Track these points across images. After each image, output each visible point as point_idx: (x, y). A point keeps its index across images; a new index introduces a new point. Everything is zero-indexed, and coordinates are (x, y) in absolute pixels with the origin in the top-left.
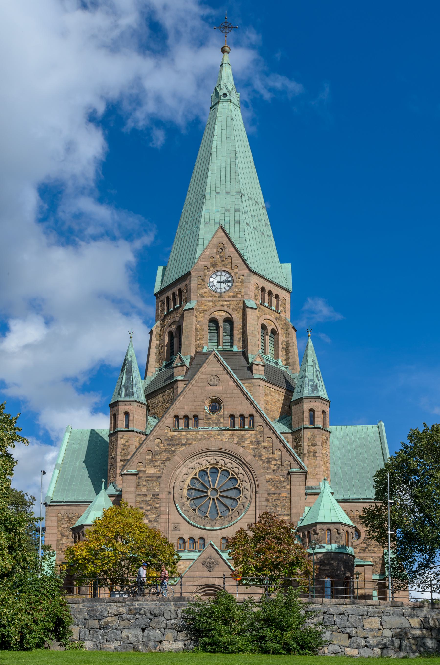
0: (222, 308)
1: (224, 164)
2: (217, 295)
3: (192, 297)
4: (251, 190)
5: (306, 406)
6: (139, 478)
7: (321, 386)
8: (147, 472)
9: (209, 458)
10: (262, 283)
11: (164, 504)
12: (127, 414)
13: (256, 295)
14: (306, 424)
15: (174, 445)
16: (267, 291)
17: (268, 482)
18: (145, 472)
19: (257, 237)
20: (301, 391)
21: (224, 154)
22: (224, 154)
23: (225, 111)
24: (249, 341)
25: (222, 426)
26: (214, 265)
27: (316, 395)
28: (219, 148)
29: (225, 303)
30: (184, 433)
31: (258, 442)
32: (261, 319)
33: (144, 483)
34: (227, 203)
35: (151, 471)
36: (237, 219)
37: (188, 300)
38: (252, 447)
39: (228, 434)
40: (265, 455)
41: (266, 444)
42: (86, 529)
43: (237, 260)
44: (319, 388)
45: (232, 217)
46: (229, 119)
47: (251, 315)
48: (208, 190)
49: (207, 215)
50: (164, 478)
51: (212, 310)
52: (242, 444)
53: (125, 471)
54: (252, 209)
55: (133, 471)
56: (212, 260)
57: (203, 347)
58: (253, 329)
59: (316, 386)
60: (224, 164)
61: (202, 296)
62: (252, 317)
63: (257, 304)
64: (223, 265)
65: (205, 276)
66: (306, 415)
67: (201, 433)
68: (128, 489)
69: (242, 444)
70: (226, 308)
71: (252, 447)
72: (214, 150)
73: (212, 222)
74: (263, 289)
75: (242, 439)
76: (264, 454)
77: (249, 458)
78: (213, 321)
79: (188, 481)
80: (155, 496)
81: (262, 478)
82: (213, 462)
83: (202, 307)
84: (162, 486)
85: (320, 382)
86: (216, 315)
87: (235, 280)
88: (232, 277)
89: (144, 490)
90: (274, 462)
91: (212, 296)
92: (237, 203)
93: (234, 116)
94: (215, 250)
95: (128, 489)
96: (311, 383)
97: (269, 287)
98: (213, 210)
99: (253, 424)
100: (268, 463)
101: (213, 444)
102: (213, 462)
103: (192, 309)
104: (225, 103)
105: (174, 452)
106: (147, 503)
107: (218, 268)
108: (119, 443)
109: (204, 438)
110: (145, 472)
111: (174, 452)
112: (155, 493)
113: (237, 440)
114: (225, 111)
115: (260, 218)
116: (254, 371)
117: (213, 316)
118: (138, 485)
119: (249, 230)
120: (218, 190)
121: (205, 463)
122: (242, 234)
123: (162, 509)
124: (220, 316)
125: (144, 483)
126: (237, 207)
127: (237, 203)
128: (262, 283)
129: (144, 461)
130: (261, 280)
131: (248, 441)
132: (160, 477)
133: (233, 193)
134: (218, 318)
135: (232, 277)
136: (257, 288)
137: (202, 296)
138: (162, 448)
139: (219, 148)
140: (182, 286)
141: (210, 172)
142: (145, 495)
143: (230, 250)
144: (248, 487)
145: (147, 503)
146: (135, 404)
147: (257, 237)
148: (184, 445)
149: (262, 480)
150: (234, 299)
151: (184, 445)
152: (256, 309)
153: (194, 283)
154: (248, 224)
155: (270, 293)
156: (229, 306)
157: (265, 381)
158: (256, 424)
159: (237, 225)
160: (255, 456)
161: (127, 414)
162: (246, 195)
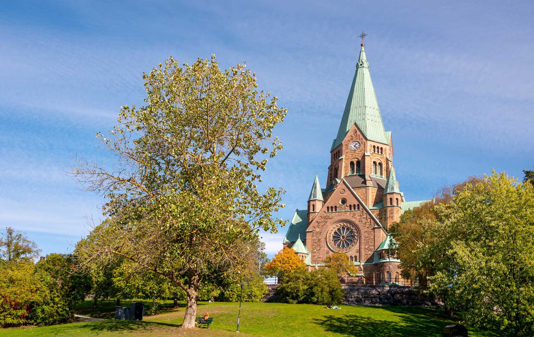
0: (356, 157)
1: (359, 95)
2: (353, 152)
3: (343, 153)
4: (371, 103)
5: (389, 197)
6: (313, 233)
7: (396, 188)
8: (316, 230)
9: (341, 224)
10: (373, 144)
11: (322, 243)
12: (313, 205)
13: (370, 150)
14: (389, 204)
15: (327, 219)
16: (376, 147)
17: (365, 232)
18: (315, 230)
19: (373, 124)
20: (387, 191)
21: (359, 90)
22: (359, 90)
23: (361, 71)
24: (366, 170)
25: (346, 210)
26: (352, 139)
27: (393, 192)
28: (357, 88)
29: (357, 155)
30: (331, 214)
31: (361, 216)
32: (373, 159)
33: (315, 235)
34: (360, 111)
35: (317, 230)
36: (363, 118)
37: (341, 155)
38: (358, 218)
39: (348, 213)
40: (364, 221)
41: (364, 216)
42: (299, 254)
43: (361, 137)
44: (394, 188)
45: (361, 117)
46: (363, 75)
47: (367, 159)
48: (352, 107)
49: (351, 118)
50: (323, 232)
51: (351, 158)
52: (354, 217)
53: (307, 231)
54: (371, 112)
55: (311, 230)
56: (351, 137)
57: (347, 174)
58: (368, 164)
59: (393, 187)
60: (359, 95)
61: (347, 153)
62: (368, 160)
63: (370, 153)
64: (356, 139)
65: (348, 144)
66: (389, 201)
67: (338, 213)
68: (309, 238)
69: (354, 217)
70: (357, 157)
71: (358, 218)
72: (355, 89)
73: (353, 120)
74: (374, 147)
75: (354, 214)
76: (363, 220)
77: (357, 223)
78: (352, 163)
79: (333, 233)
80: (319, 240)
81: (363, 231)
82: (343, 225)
83: (347, 157)
84: (322, 236)
85: (396, 186)
86: (353, 160)
87: (361, 144)
88: (359, 143)
89: (315, 238)
90: (368, 224)
91: (351, 152)
92: (364, 111)
93: (365, 73)
94: (353, 133)
95: (309, 238)
96: (391, 187)
97: (377, 145)
98: (353, 115)
99: (358, 208)
100: (365, 224)
101: (343, 217)
102: (343, 225)
103: (342, 159)
104: (361, 68)
105: (327, 222)
106: (316, 243)
107: (354, 140)
108: (310, 217)
109: (339, 215)
110: (315, 230)
111: (327, 222)
112: (319, 239)
113: (352, 215)
114: (361, 71)
115: (375, 115)
116: (367, 183)
117: (352, 160)
118: (313, 236)
119: (369, 122)
120: (356, 106)
121: (339, 225)
122: (365, 124)
123: (322, 245)
124: (355, 160)
125: (315, 235)
126: (364, 113)
127: (364, 111)
128: (373, 144)
129: (315, 226)
130: (373, 142)
131: (357, 216)
132: (321, 232)
133: (362, 107)
134: (354, 161)
135: (359, 143)
136: (371, 146)
137: (347, 153)
138: (322, 220)
139: (357, 88)
140: (338, 149)
141: (353, 99)
142: (315, 240)
143: (358, 133)
144: (357, 235)
145: (316, 243)
146: (317, 201)
147: (373, 124)
148: (331, 219)
149: (362, 232)
150: (361, 152)
151: (331, 219)
152: (369, 156)
153: (344, 148)
154: (368, 119)
155: (378, 148)
156: (358, 156)
157: (372, 187)
158: (360, 208)
159: (363, 121)
160: (359, 221)
161: (313, 205)
162: (368, 106)
